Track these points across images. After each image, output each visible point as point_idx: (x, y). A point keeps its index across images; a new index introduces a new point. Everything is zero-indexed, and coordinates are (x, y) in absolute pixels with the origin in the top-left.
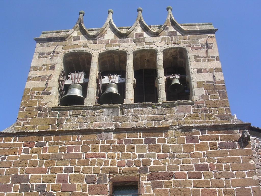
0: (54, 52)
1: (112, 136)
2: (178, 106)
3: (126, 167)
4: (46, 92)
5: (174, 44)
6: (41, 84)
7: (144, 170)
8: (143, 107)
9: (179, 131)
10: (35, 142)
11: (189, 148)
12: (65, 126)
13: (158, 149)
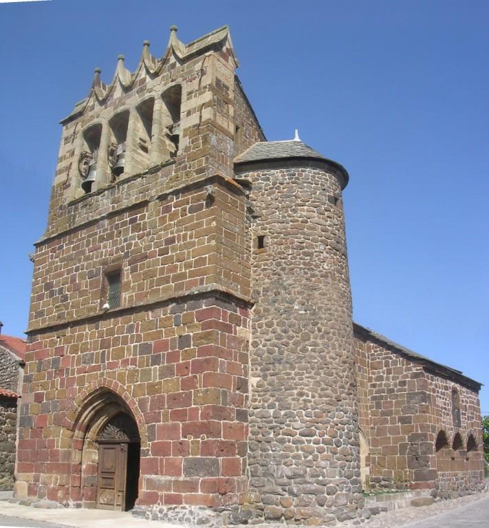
0: (74, 133)
1: (106, 222)
2: (163, 169)
3: (114, 255)
4: (66, 185)
5: (172, 81)
6: (62, 178)
7: (126, 255)
8: (134, 180)
9: (158, 201)
10: (155, 425)
11: (163, 220)
12: (80, 221)
13: (139, 228)
